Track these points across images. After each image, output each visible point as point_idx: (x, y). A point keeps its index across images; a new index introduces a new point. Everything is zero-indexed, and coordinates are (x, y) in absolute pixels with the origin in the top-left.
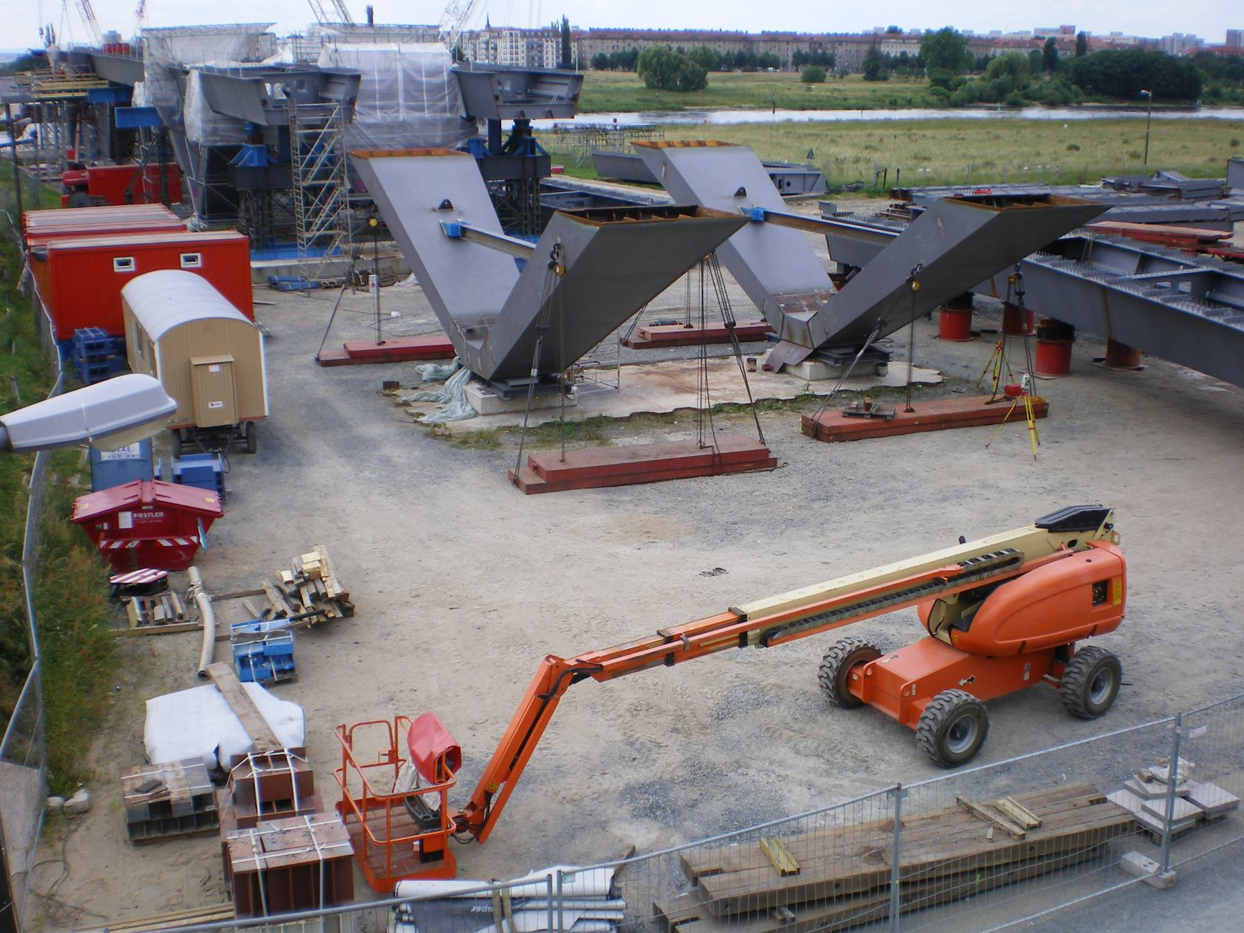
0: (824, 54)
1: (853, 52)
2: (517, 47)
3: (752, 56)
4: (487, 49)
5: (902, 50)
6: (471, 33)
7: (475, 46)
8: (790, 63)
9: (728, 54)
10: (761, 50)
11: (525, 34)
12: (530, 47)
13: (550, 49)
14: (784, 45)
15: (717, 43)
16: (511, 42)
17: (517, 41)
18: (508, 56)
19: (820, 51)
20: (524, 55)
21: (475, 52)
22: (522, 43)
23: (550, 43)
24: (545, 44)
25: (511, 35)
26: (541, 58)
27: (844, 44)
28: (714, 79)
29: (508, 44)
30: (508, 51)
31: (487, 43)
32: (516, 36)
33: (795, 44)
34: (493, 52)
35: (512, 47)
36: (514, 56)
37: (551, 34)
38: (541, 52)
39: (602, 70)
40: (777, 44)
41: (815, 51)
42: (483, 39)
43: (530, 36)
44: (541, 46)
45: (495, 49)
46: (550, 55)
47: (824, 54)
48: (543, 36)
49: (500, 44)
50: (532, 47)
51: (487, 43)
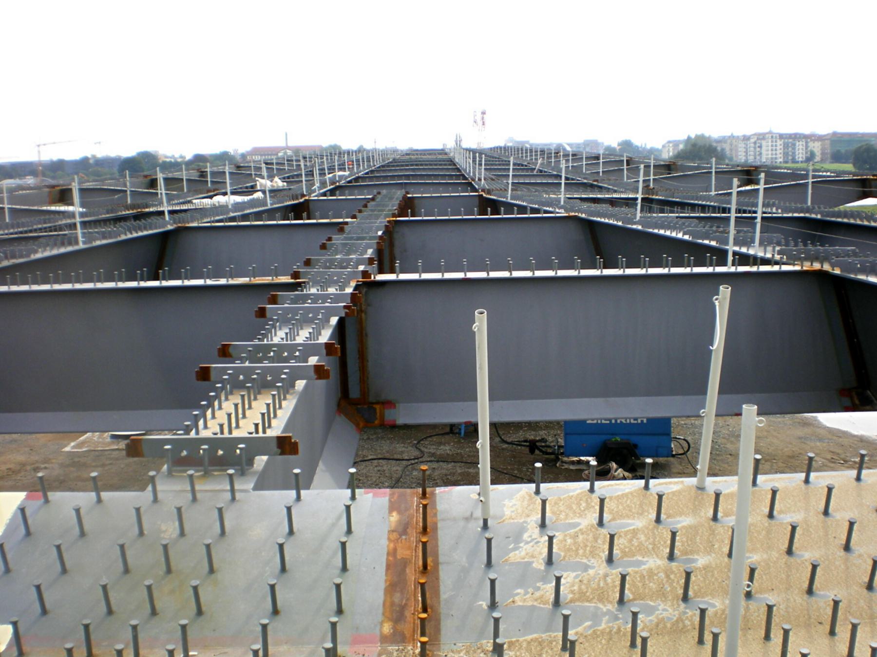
2: (776, 146)
4: (755, 148)
6: (744, 136)
7: (747, 145)
11: (781, 136)
12: (786, 146)
13: (801, 147)
16: (772, 142)
17: (776, 142)
18: (770, 152)
21: (747, 149)
22: (780, 143)
23: (801, 143)
24: (797, 144)
26: (794, 153)
29: (770, 144)
30: (770, 148)
32: (776, 138)
34: (758, 149)
36: (774, 152)
38: (794, 149)
42: (752, 140)
43: (786, 138)
44: (794, 145)
45: (760, 147)
46: (801, 151)
49: (764, 143)
50: (788, 145)
51: (755, 143)
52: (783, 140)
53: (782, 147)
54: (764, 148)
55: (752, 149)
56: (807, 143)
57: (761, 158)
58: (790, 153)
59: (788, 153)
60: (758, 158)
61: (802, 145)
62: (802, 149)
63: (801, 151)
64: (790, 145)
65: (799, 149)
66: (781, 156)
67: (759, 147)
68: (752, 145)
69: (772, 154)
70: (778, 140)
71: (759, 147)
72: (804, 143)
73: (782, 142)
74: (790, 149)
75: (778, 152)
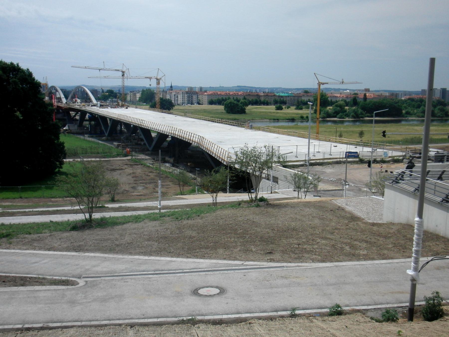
0: (283, 100)
1: (293, 99)
2: (184, 97)
3: (260, 100)
5: (308, 98)
7: (171, 96)
8: (272, 103)
9: (252, 100)
10: (262, 99)
12: (189, 97)
13: (195, 98)
14: (270, 97)
15: (249, 96)
16: (183, 95)
17: (184, 95)
18: (182, 100)
19: (282, 99)
20: (187, 99)
22: (186, 95)
23: (195, 96)
24: (193, 96)
25: (183, 93)
26: (192, 101)
27: (290, 97)
28: (249, 108)
29: (181, 96)
30: (182, 98)
31: (175, 95)
33: (274, 97)
34: (176, 98)
35: (183, 97)
37: (195, 93)
39: (212, 105)
40: (268, 97)
41: (280, 99)
43: (189, 94)
44: (192, 97)
45: (177, 97)
46: (195, 100)
47: (283, 100)
48: (193, 93)
49: (179, 96)
50: (189, 97)
51: (175, 95)
52: (187, 95)
53: (187, 97)
54: (179, 98)
55: (173, 98)
56: (197, 96)
57: (177, 102)
58: (190, 100)
59: (189, 100)
60: (176, 102)
61: (196, 97)
62: (196, 99)
63: (195, 100)
64: (190, 97)
65: (194, 99)
66: (187, 101)
67: (176, 97)
68: (173, 96)
69: (183, 101)
70: (185, 94)
71: (176, 97)
72: (196, 96)
73: (187, 96)
74: (190, 98)
75: (185, 100)
